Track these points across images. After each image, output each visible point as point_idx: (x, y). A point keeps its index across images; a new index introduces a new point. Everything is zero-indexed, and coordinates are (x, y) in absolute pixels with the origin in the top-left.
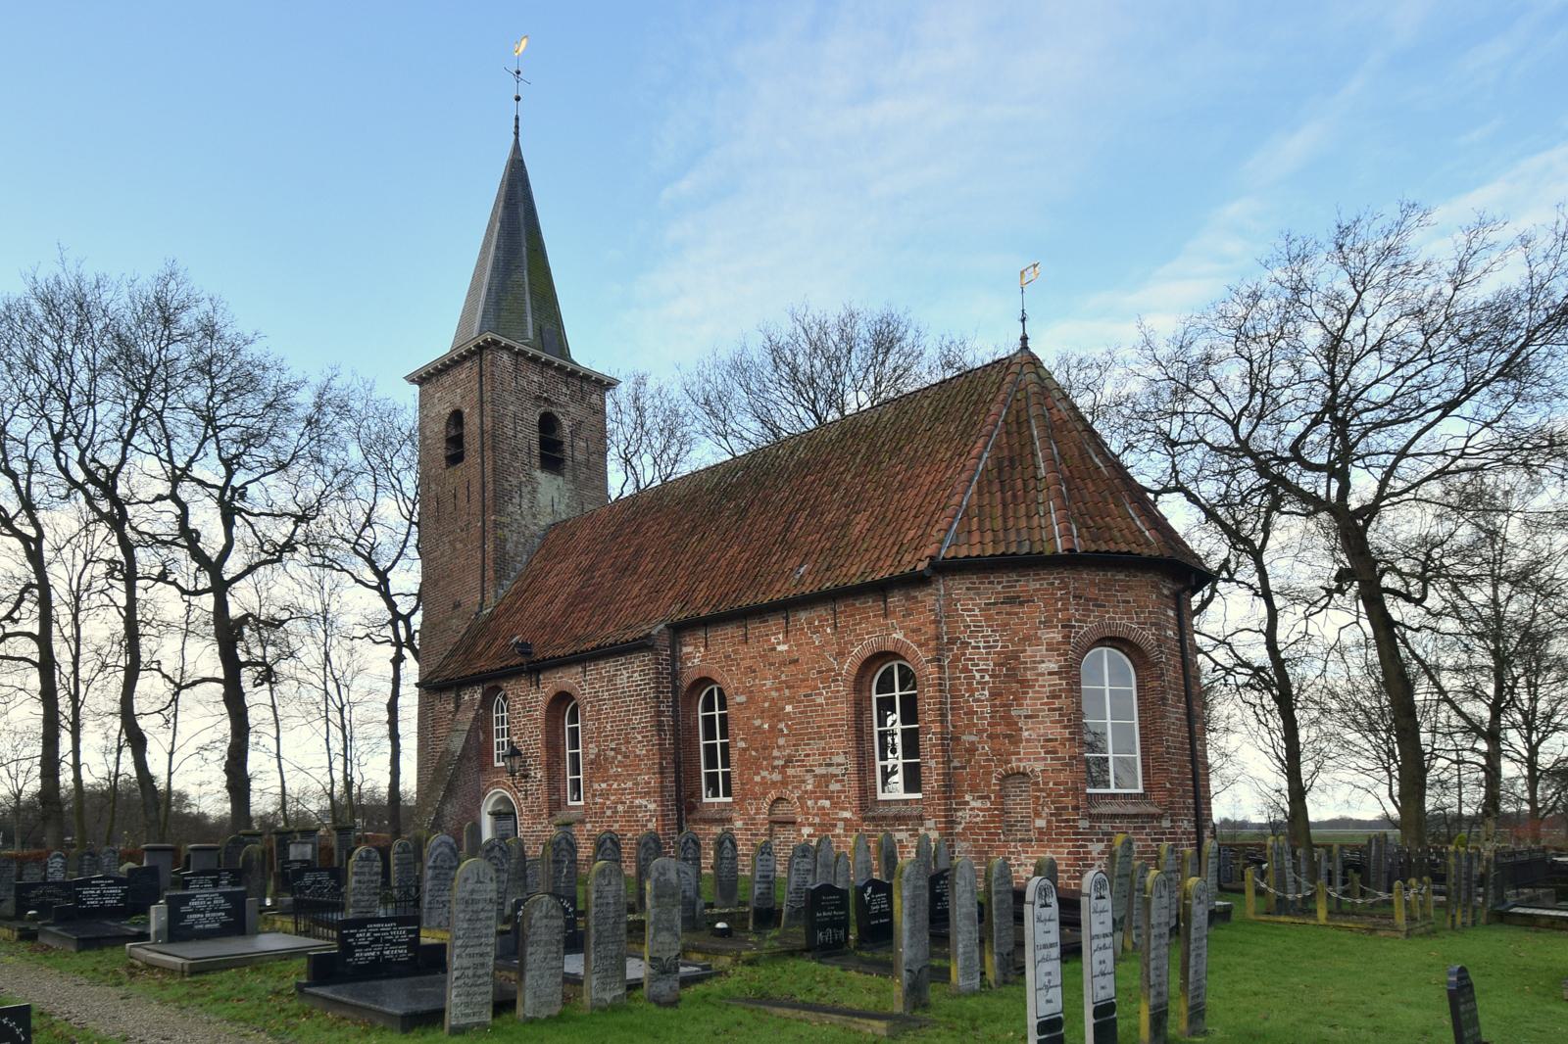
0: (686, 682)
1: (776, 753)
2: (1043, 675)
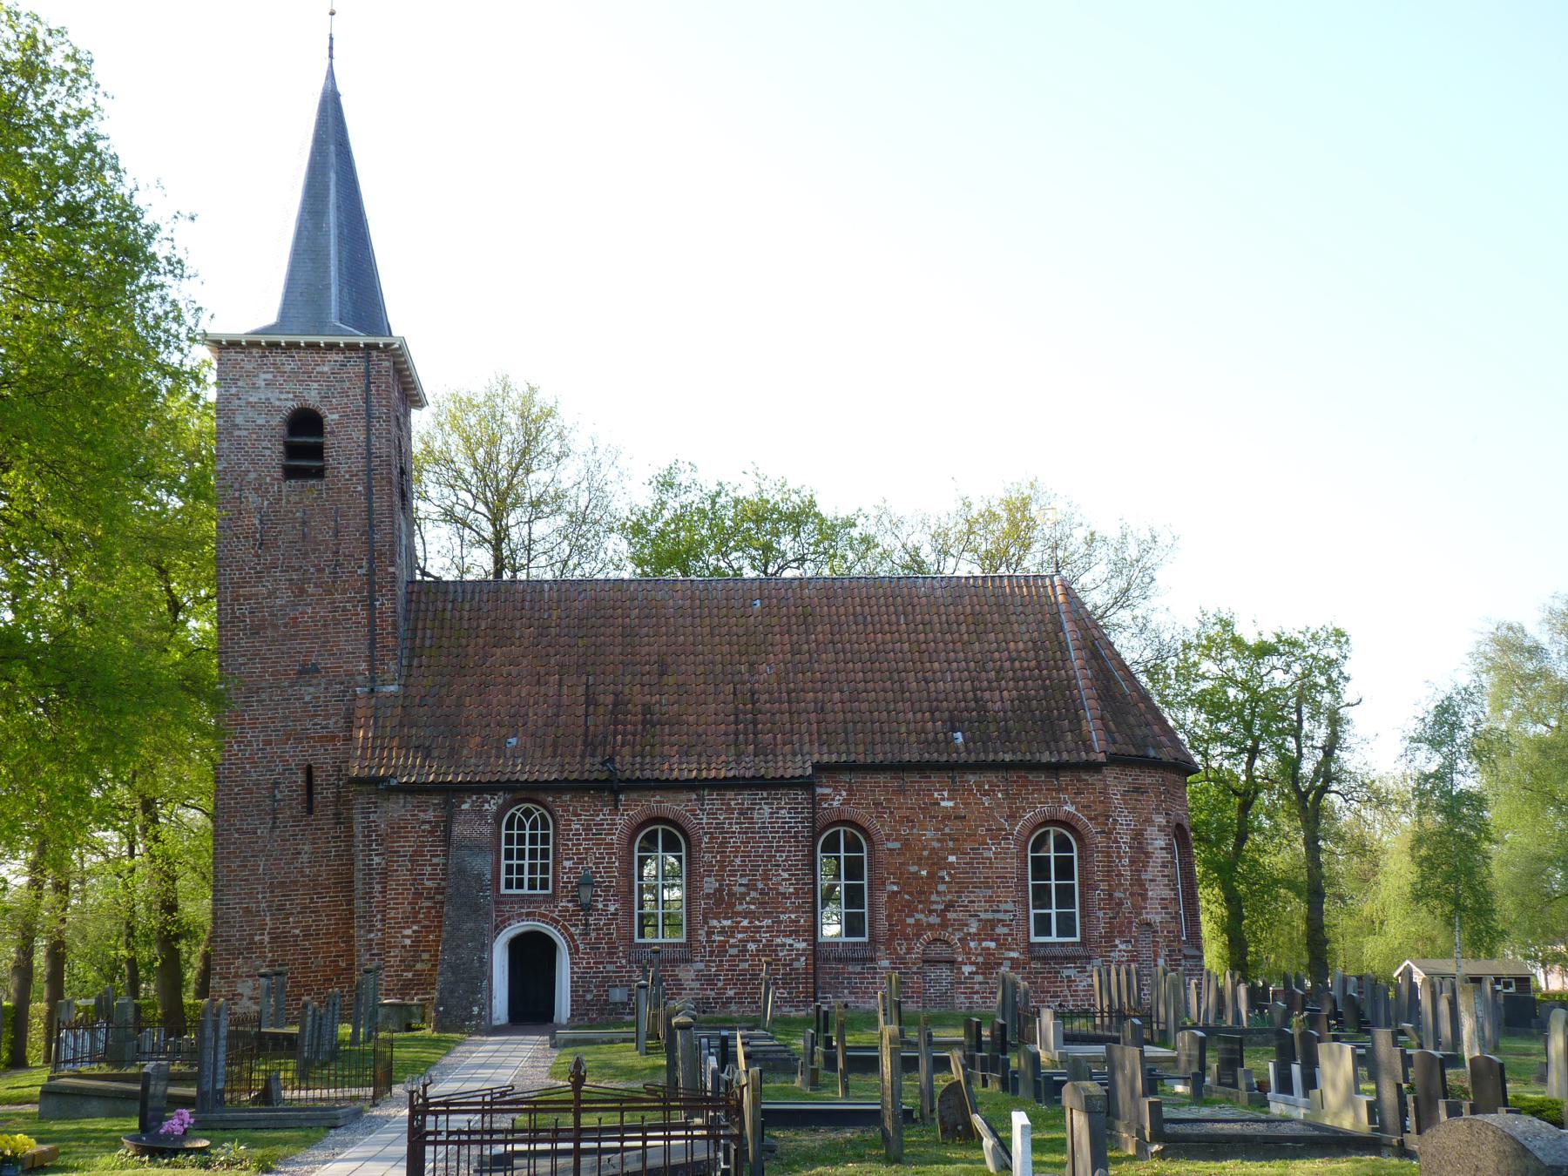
1: (934, 898)
2: (1156, 849)
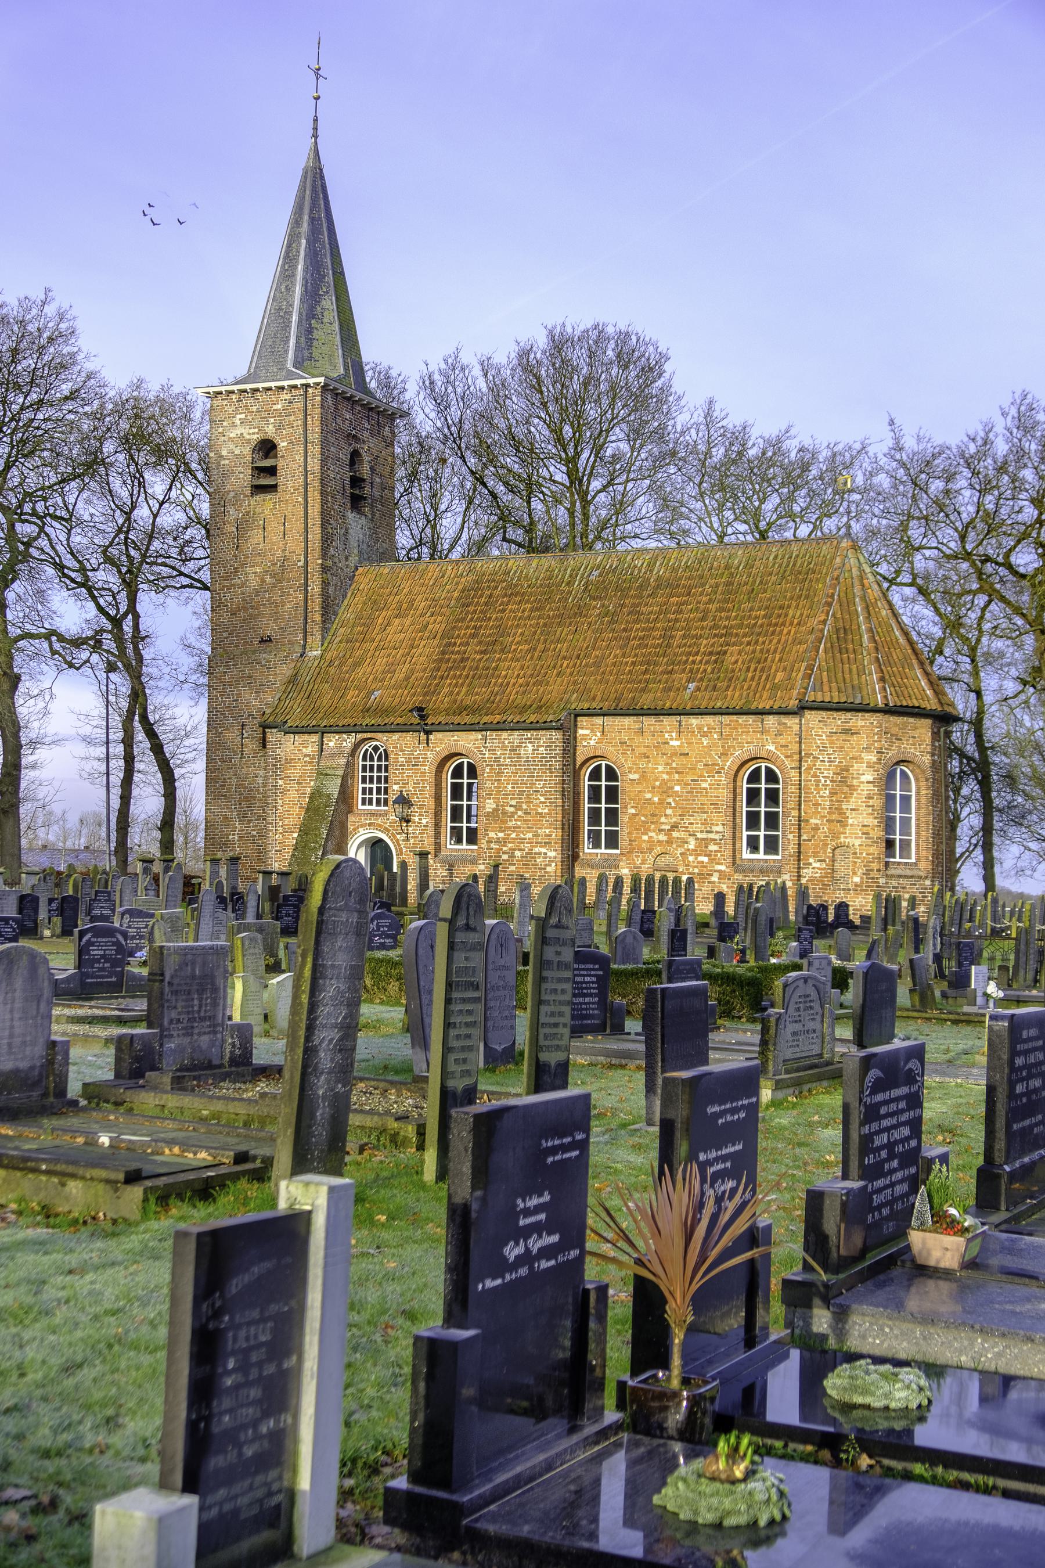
0: (579, 760)
1: (663, 819)
